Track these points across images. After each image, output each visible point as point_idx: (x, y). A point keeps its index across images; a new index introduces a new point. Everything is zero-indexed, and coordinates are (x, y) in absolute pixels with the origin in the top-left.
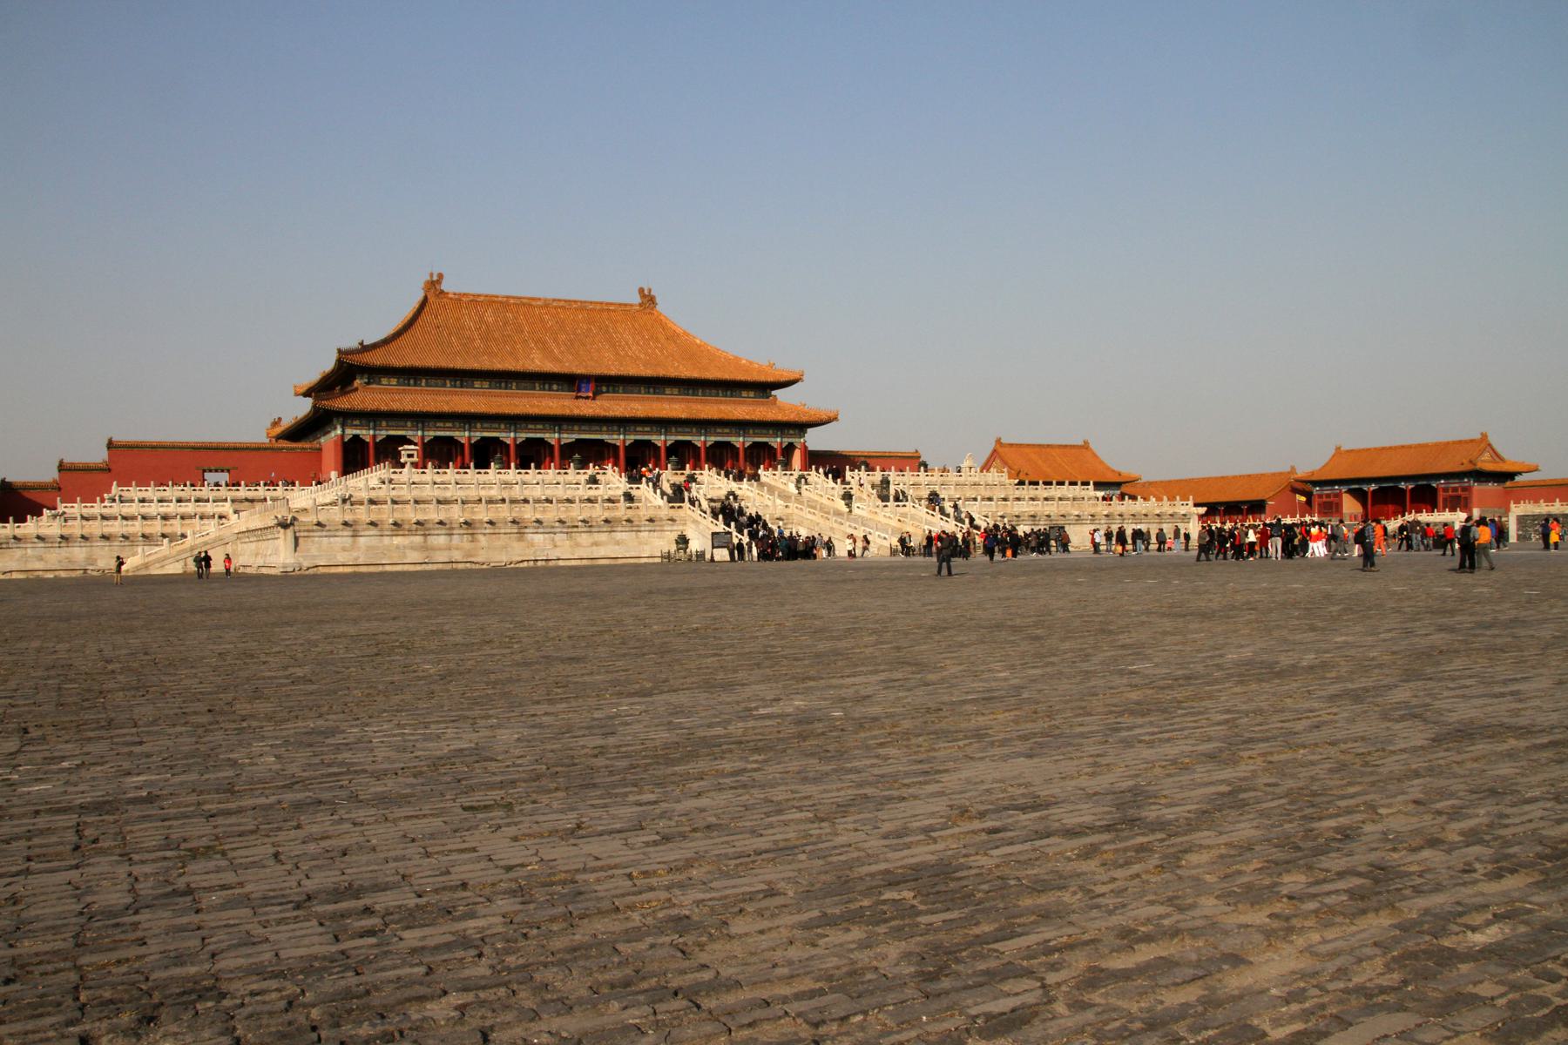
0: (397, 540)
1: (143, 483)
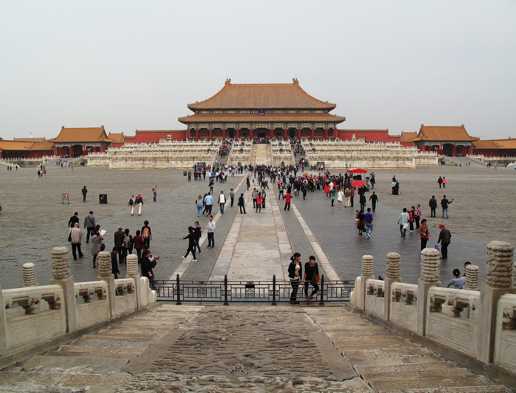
0: (137, 162)
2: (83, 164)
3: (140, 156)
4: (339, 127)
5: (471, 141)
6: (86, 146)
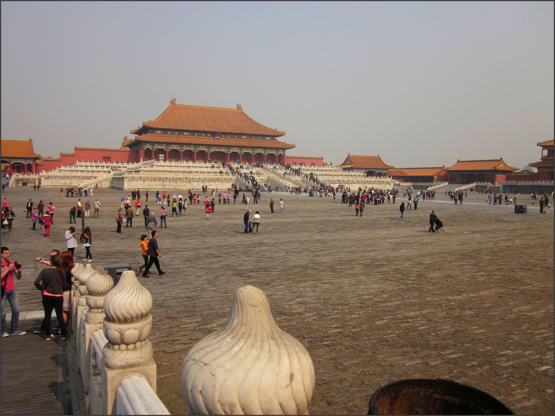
0: (155, 182)
1: (86, 161)
4: (288, 153)
5: (387, 169)
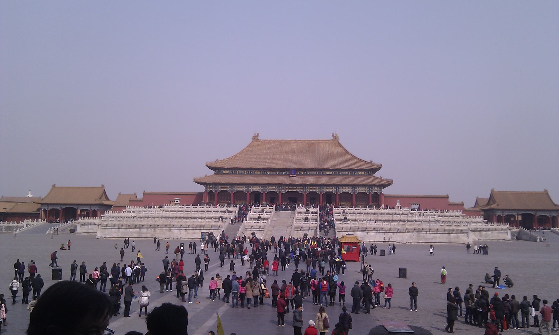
0: (131, 230)
2: (73, 231)
3: (136, 223)
4: (386, 191)
6: (80, 208)
